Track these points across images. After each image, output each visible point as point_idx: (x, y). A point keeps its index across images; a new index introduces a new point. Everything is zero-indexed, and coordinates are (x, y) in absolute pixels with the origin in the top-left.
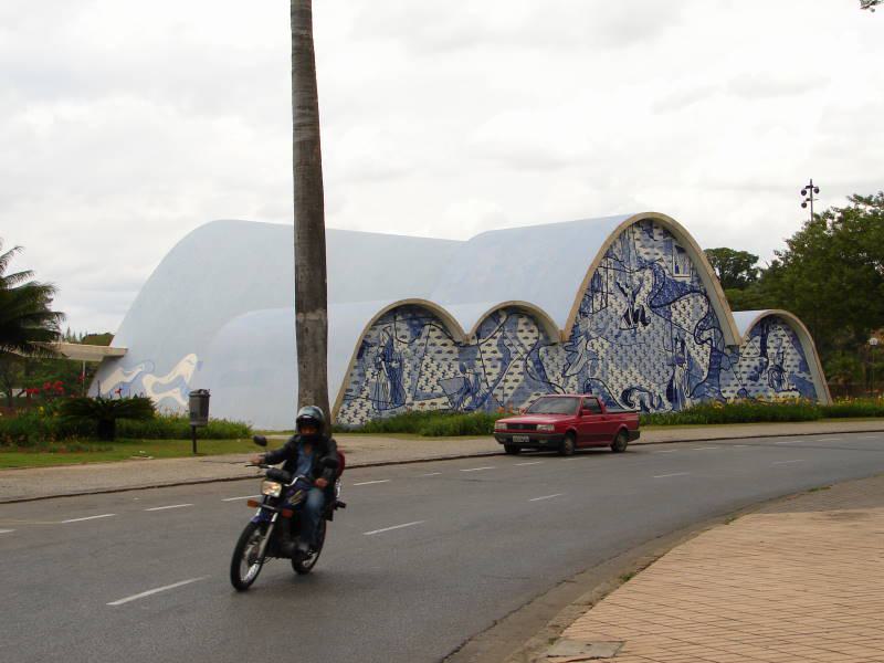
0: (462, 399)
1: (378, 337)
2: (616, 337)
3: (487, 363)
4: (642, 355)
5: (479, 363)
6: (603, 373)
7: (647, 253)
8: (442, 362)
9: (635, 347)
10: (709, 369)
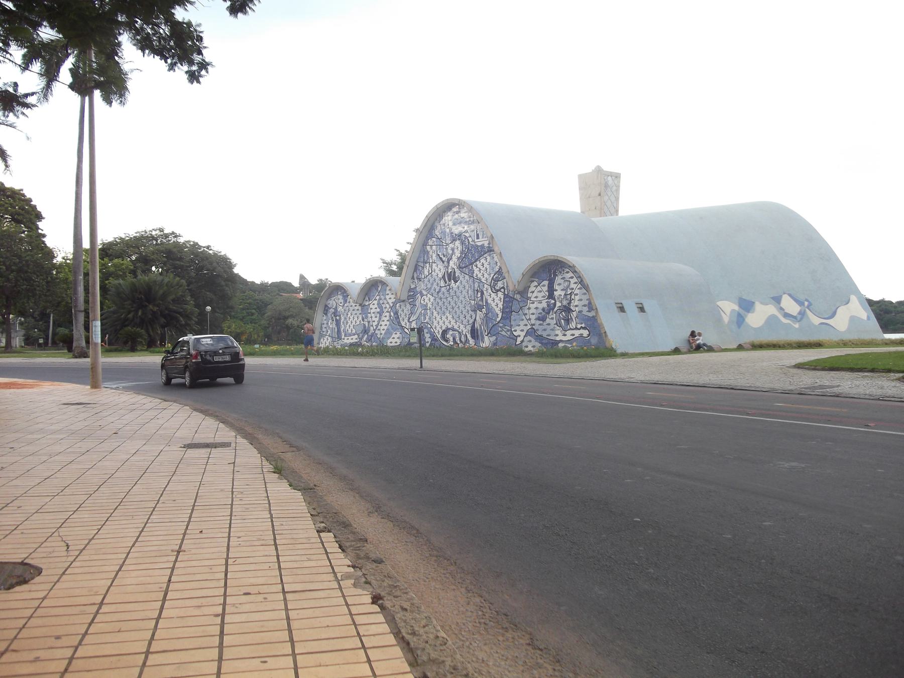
0: (363, 337)
2: (438, 292)
3: (373, 315)
4: (454, 305)
5: (369, 315)
9: (449, 299)
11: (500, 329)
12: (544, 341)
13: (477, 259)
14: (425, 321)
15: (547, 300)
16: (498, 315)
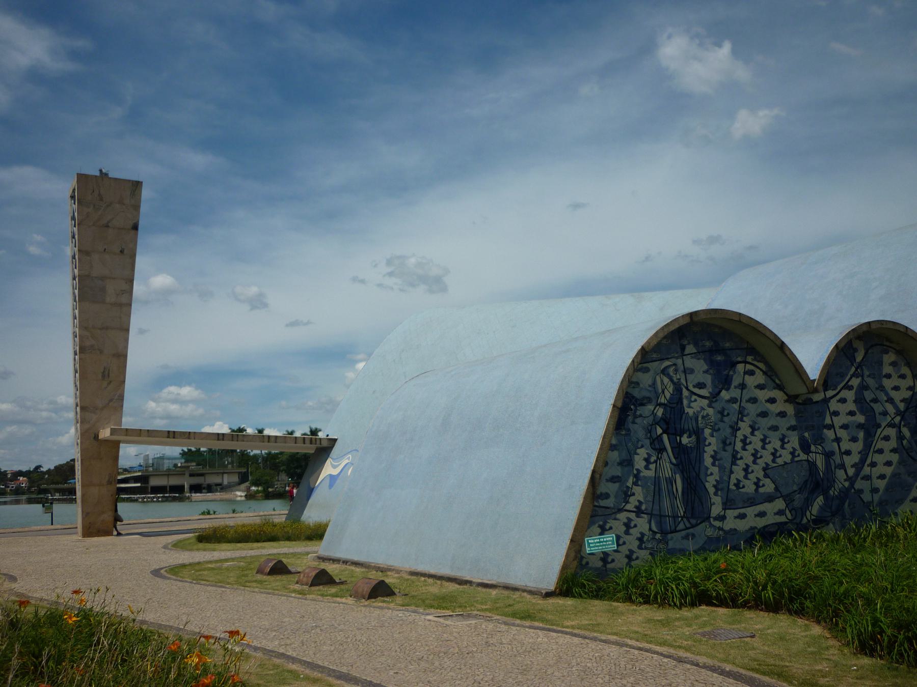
0: (808, 503)
1: (654, 383)
5: (830, 434)
8: (771, 433)
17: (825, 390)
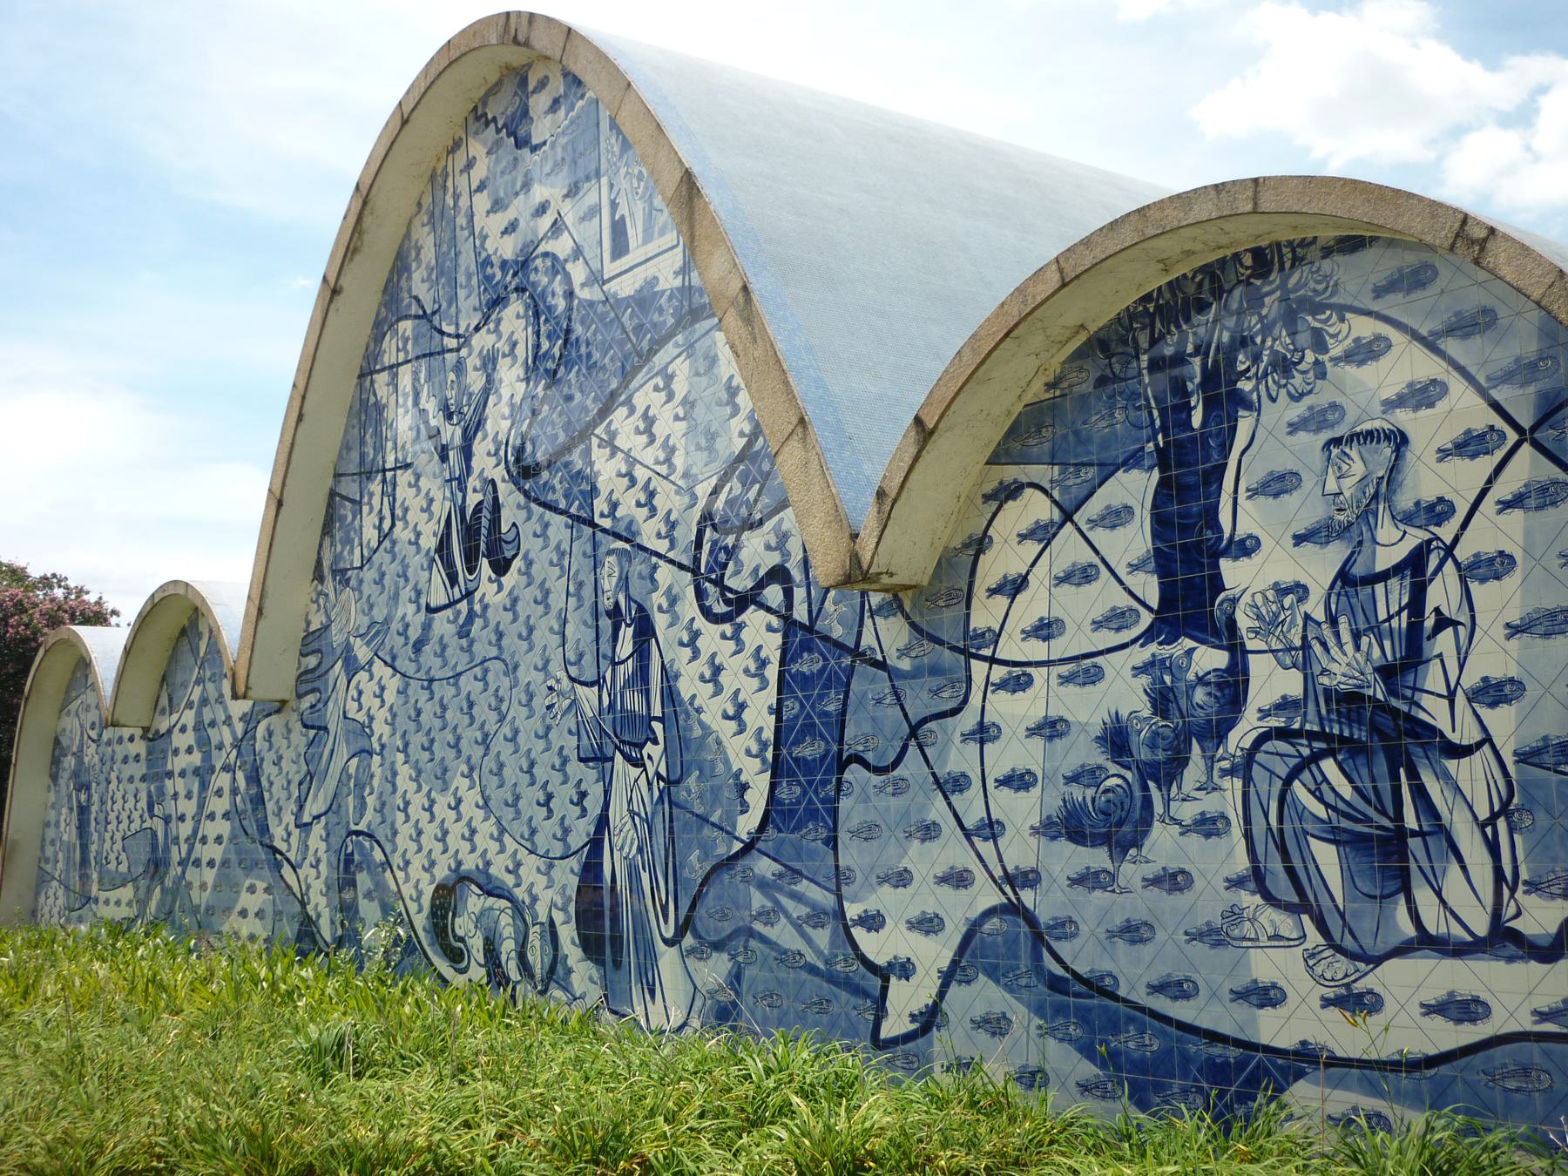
0: (149, 891)
2: (418, 646)
6: (380, 810)
7: (511, 228)
10: (778, 770)
11: (758, 900)
12: (1129, 1042)
13: (613, 395)
14: (362, 827)
15: (1141, 654)
16: (743, 788)
17: (171, 714)
